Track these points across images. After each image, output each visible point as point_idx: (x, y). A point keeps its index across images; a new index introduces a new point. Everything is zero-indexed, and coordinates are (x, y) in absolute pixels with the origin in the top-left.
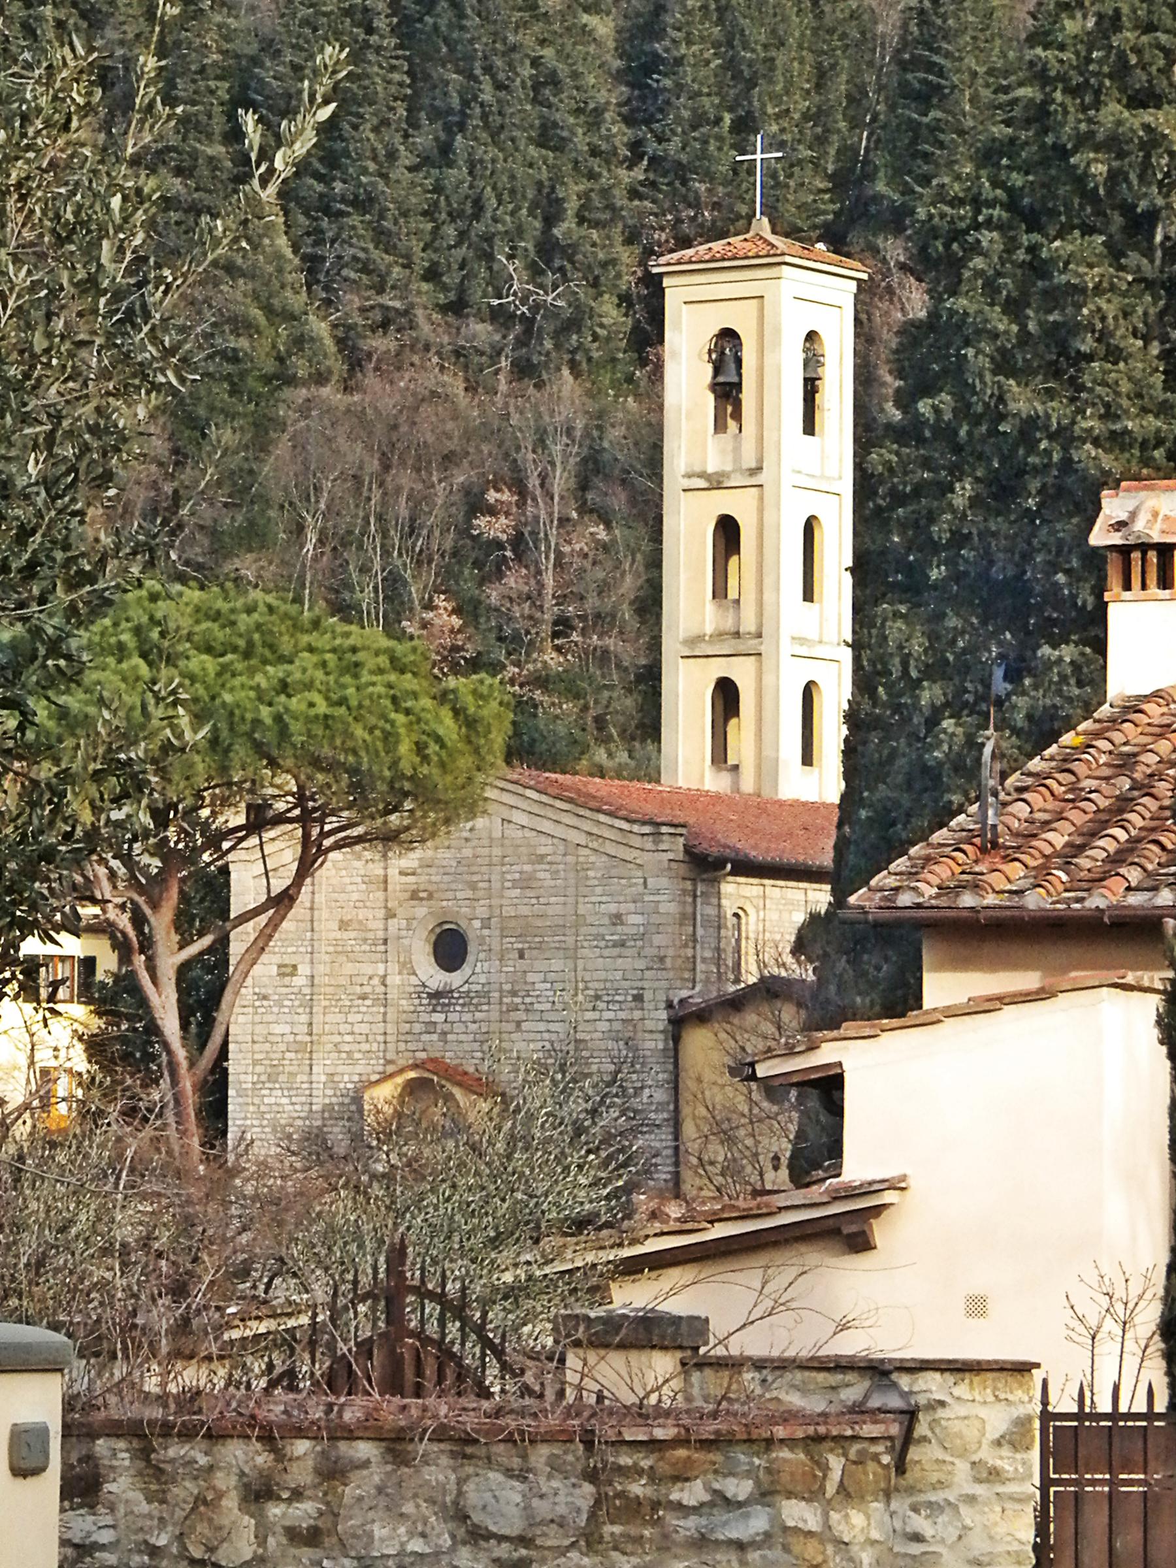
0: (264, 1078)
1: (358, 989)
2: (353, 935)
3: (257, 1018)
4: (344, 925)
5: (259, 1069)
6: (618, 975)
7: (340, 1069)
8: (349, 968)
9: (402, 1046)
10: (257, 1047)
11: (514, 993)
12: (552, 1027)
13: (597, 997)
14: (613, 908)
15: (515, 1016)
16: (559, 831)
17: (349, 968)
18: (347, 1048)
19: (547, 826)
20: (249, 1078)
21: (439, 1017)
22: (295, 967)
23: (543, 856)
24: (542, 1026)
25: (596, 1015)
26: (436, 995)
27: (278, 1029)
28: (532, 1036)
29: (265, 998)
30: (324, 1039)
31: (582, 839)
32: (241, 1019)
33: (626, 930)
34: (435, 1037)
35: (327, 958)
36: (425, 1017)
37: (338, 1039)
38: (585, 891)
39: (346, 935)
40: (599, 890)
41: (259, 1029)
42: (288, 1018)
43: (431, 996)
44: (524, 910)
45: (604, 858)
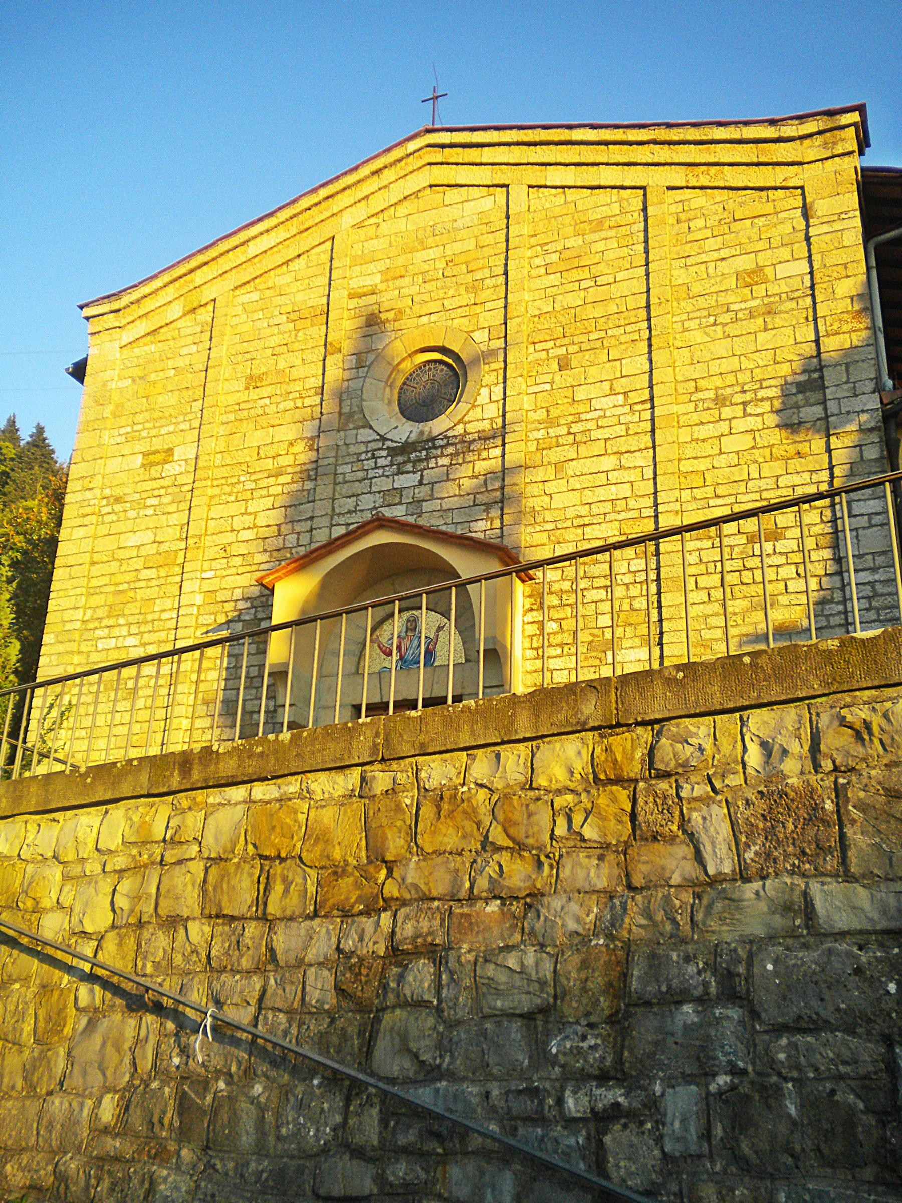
0: (101, 613)
1: (269, 464)
3: (103, 530)
4: (253, 382)
6: (763, 359)
7: (229, 582)
8: (256, 438)
10: (96, 570)
11: (550, 422)
12: (626, 460)
13: (720, 401)
14: (745, 263)
15: (554, 455)
17: (256, 438)
19: (608, 176)
20: (79, 614)
22: (170, 451)
23: (601, 221)
24: (608, 462)
25: (724, 427)
26: (406, 448)
27: (132, 540)
28: (587, 481)
29: (118, 500)
30: (208, 541)
31: (677, 177)
32: (79, 533)
33: (773, 289)
35: (223, 430)
36: (384, 484)
38: (688, 249)
39: (254, 394)
40: (711, 243)
43: (393, 452)
44: (574, 300)
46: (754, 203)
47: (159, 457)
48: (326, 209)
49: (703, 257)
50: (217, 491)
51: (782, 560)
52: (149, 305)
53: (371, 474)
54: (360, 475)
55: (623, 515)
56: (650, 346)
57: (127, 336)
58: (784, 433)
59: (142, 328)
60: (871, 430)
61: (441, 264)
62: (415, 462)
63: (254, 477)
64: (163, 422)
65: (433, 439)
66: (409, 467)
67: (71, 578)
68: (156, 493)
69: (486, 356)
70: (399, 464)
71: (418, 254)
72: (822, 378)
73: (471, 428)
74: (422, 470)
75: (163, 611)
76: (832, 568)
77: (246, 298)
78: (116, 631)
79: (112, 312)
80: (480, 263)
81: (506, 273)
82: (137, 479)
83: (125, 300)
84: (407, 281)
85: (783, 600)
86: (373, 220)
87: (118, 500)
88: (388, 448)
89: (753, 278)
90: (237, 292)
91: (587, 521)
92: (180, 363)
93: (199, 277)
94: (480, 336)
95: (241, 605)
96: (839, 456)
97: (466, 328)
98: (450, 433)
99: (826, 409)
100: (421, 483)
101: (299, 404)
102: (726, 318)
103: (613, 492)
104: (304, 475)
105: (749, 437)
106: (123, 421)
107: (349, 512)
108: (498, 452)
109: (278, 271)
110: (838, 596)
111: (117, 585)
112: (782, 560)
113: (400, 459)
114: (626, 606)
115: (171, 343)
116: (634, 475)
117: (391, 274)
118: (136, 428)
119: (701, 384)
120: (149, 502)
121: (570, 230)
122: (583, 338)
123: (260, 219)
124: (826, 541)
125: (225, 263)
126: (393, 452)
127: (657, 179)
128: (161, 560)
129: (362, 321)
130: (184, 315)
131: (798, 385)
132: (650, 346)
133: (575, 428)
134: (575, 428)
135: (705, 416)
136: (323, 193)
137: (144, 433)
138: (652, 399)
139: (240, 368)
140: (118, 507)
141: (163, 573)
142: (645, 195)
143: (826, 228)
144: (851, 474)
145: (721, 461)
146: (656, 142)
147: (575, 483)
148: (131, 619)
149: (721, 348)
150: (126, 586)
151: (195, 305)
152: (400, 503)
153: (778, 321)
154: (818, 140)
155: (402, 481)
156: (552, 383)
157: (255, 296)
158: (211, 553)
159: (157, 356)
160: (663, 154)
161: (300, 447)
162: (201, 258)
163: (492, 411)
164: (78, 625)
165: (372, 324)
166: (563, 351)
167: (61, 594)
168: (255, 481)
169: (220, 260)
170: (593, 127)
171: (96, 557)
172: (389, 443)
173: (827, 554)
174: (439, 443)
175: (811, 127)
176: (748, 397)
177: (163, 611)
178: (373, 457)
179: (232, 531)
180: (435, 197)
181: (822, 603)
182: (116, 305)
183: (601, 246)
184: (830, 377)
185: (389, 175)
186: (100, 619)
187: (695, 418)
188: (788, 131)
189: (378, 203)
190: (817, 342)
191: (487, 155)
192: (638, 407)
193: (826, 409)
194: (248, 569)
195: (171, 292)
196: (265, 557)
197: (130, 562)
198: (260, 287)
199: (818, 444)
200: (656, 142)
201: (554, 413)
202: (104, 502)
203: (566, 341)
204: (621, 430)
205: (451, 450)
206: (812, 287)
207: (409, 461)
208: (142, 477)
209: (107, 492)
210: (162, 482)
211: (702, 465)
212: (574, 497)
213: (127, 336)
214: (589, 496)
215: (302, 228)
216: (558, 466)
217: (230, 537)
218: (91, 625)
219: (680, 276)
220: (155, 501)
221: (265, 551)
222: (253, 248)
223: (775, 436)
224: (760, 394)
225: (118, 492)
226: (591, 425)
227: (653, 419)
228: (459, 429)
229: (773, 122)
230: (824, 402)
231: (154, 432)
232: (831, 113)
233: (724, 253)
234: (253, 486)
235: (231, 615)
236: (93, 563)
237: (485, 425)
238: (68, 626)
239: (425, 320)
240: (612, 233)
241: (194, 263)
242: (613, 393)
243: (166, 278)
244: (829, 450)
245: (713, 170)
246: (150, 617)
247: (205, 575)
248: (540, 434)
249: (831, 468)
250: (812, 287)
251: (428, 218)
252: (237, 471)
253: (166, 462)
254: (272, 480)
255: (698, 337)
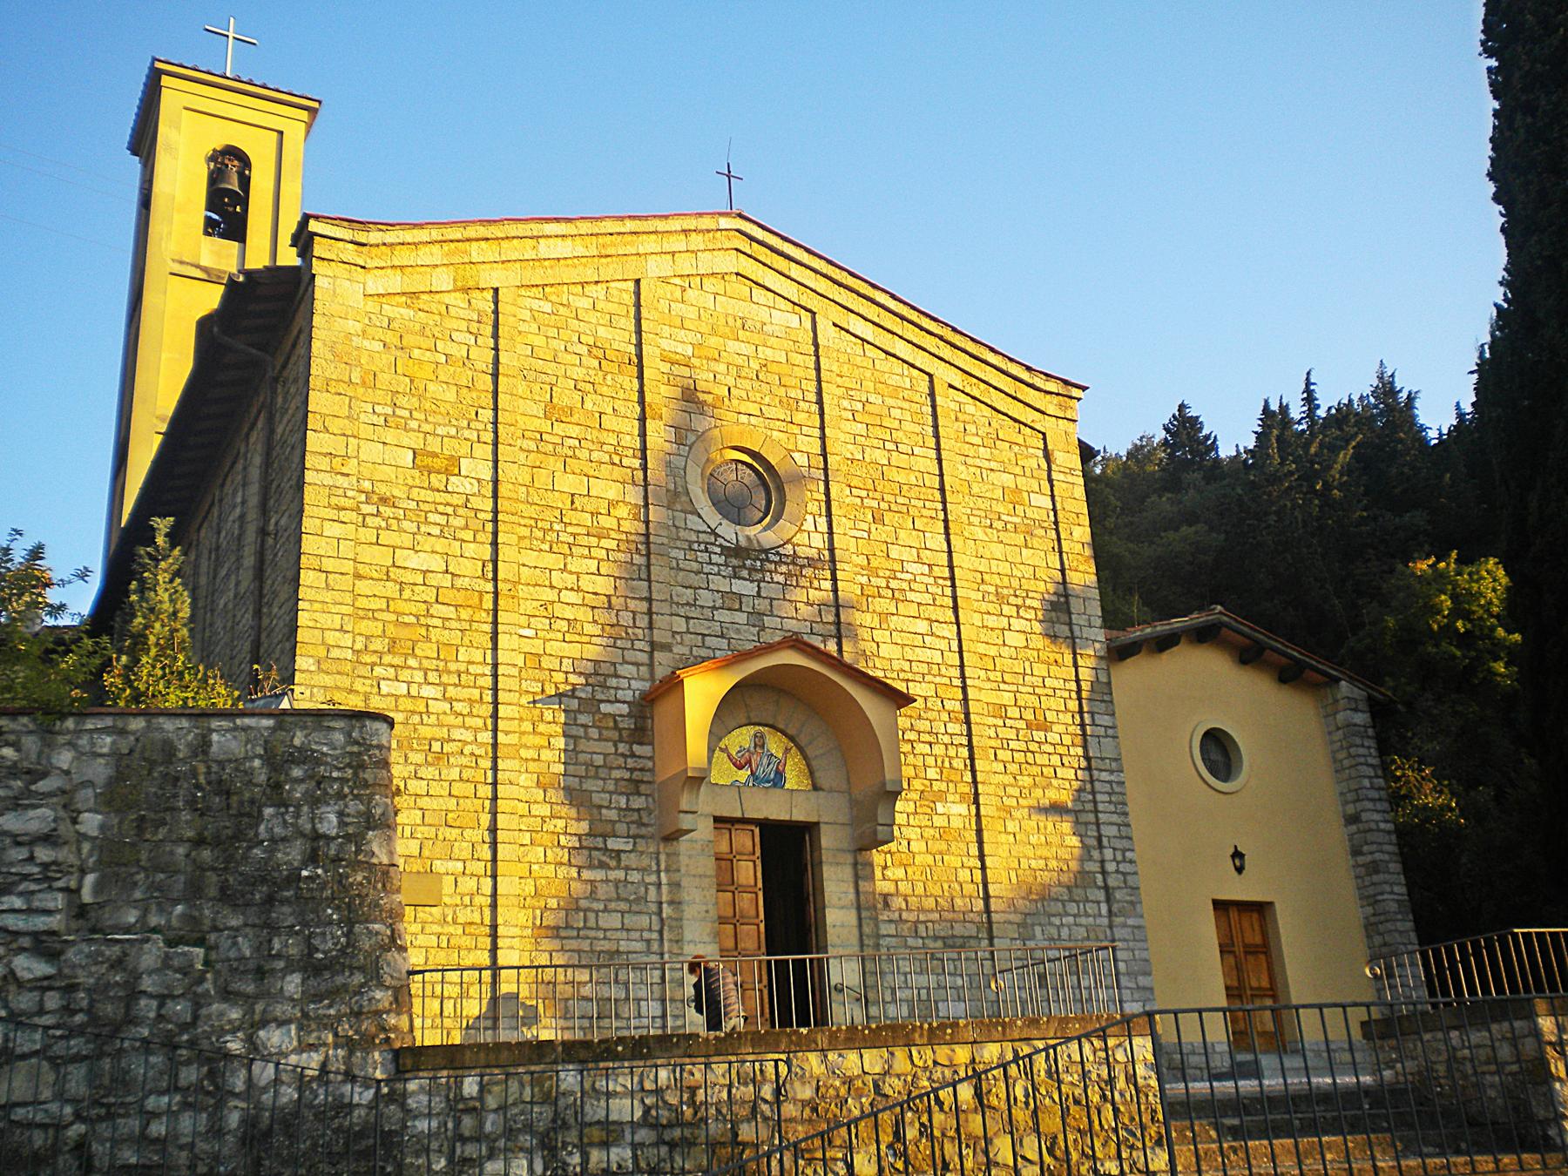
0: (377, 645)
2: (574, 431)
4: (552, 411)
5: (366, 627)
7: (553, 647)
8: (568, 483)
9: (680, 624)
10: (363, 587)
16: (921, 360)
17: (568, 483)
18: (569, 613)
20: (347, 640)
21: (745, 587)
22: (455, 461)
24: (922, 627)
34: (741, 618)
37: (550, 595)
41: (367, 554)
42: (440, 545)
43: (726, 551)
45: (987, 411)
46: (1008, 430)
47: (439, 463)
48: (631, 243)
49: (977, 462)
50: (526, 532)
51: (1051, 749)
52: (403, 257)
53: (707, 569)
54: (695, 566)
55: (938, 680)
56: (947, 528)
57: (376, 283)
58: (1047, 641)
59: (394, 282)
60: (1101, 658)
61: (755, 365)
62: (752, 570)
63: (569, 529)
64: (439, 419)
65: (766, 551)
66: (745, 573)
67: (328, 587)
68: (441, 508)
69: (800, 479)
70: (734, 567)
71: (731, 343)
72: (1067, 602)
73: (801, 551)
74: (759, 581)
75: (469, 663)
76: (1084, 764)
77: (536, 304)
78: (405, 675)
79: (352, 242)
80: (793, 382)
81: (820, 402)
82: (410, 482)
83: (374, 237)
84: (722, 368)
85: (1055, 782)
86: (678, 281)
87: (384, 500)
88: (720, 546)
89: (1014, 497)
90: (523, 292)
91: (910, 676)
92: (452, 349)
93: (476, 251)
94: (801, 460)
95: (573, 679)
96: (1085, 674)
97: (791, 447)
98: (781, 550)
99: (1071, 630)
100: (759, 595)
101: (616, 459)
102: (999, 525)
103: (925, 655)
104: (633, 547)
105: (1023, 637)
106: (379, 396)
107: (688, 604)
108: (827, 585)
109: (573, 289)
110: (1088, 786)
111: (398, 614)
112: (1051, 749)
113: (734, 562)
114: (947, 764)
115: (437, 318)
116: (943, 645)
117: (704, 352)
118: (398, 412)
119: (986, 577)
120: (432, 517)
121: (869, 385)
122: (891, 498)
123: (557, 220)
124: (1078, 740)
125: (512, 250)
126: (726, 551)
127: (944, 374)
128: (460, 598)
129: (677, 392)
130: (455, 291)
131: (1052, 603)
132: (947, 528)
133: (893, 584)
134: (893, 584)
135: (991, 608)
136: (630, 225)
137: (414, 424)
138: (952, 578)
139: (536, 388)
140: (387, 511)
141: (465, 614)
142: (931, 381)
143: (1061, 477)
144: (1092, 691)
145: (1005, 652)
146: (941, 338)
147: (897, 637)
148: (426, 663)
149: (998, 551)
150: (413, 620)
151: (471, 284)
152: (740, 610)
153: (1035, 542)
154: (1056, 399)
155: (739, 586)
156: (869, 533)
157: (547, 307)
158: (529, 607)
159: (417, 327)
160: (946, 352)
161: (622, 511)
162: (482, 231)
163: (819, 541)
164: (349, 654)
165: (690, 398)
166: (874, 504)
167: (317, 606)
168: (574, 535)
169: (505, 244)
170: (893, 297)
171: (362, 570)
172: (720, 541)
173: (1080, 751)
174: (772, 557)
175: (1052, 386)
176: (1019, 601)
177: (469, 663)
178: (706, 550)
179: (552, 587)
180: (743, 288)
181: (1079, 791)
182: (361, 237)
183: (896, 413)
184: (1076, 605)
185: (696, 241)
186: (381, 654)
187: (984, 607)
188: (1039, 381)
189: (685, 265)
190: (1063, 571)
191: (795, 271)
192: (941, 582)
193: (1071, 630)
194: (577, 638)
195: (435, 254)
196: (597, 630)
197: (416, 588)
198: (553, 298)
199: (1069, 658)
200: (941, 338)
201: (874, 563)
202: (363, 498)
203: (877, 495)
204: (928, 598)
205: (784, 569)
206: (1056, 523)
207: (744, 566)
208: (417, 482)
209: (367, 485)
210: (439, 497)
211: (993, 651)
212: (895, 652)
213: (376, 283)
214: (909, 654)
215: (604, 252)
216: (884, 616)
217: (550, 595)
218: (367, 659)
219: (964, 473)
220: (442, 520)
221: (595, 622)
222: (547, 249)
223: (1038, 642)
224: (1028, 602)
225: (382, 489)
226: (905, 586)
227: (955, 598)
228: (789, 549)
229: (1029, 369)
230: (1070, 624)
231: (427, 428)
232: (1066, 382)
233: (993, 465)
234: (571, 540)
235: (562, 688)
236: (358, 576)
237: (813, 553)
238: (335, 653)
239: (744, 418)
240: (906, 405)
241: (471, 232)
242: (919, 561)
243: (435, 234)
244: (1076, 666)
245: (982, 385)
246: (453, 667)
247: (522, 632)
248: (864, 580)
249: (1078, 681)
250: (1056, 523)
251: (742, 308)
252: (549, 515)
253: (448, 473)
254: (594, 541)
255: (980, 534)
